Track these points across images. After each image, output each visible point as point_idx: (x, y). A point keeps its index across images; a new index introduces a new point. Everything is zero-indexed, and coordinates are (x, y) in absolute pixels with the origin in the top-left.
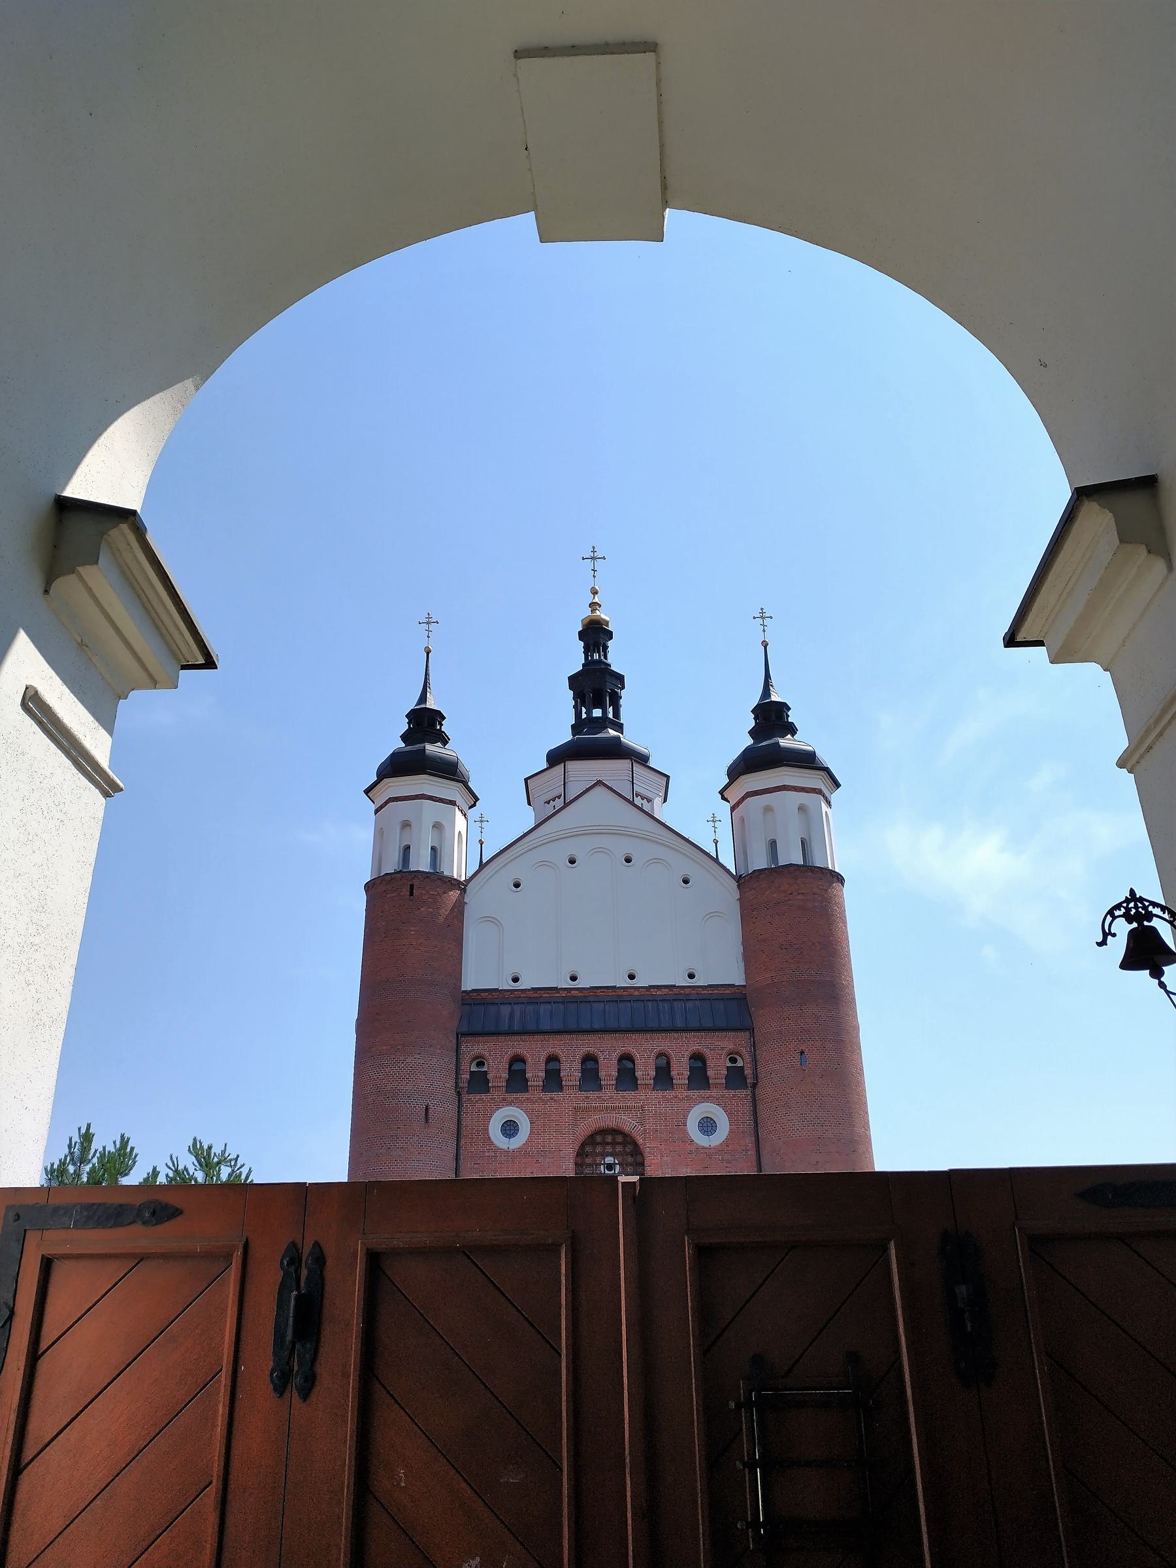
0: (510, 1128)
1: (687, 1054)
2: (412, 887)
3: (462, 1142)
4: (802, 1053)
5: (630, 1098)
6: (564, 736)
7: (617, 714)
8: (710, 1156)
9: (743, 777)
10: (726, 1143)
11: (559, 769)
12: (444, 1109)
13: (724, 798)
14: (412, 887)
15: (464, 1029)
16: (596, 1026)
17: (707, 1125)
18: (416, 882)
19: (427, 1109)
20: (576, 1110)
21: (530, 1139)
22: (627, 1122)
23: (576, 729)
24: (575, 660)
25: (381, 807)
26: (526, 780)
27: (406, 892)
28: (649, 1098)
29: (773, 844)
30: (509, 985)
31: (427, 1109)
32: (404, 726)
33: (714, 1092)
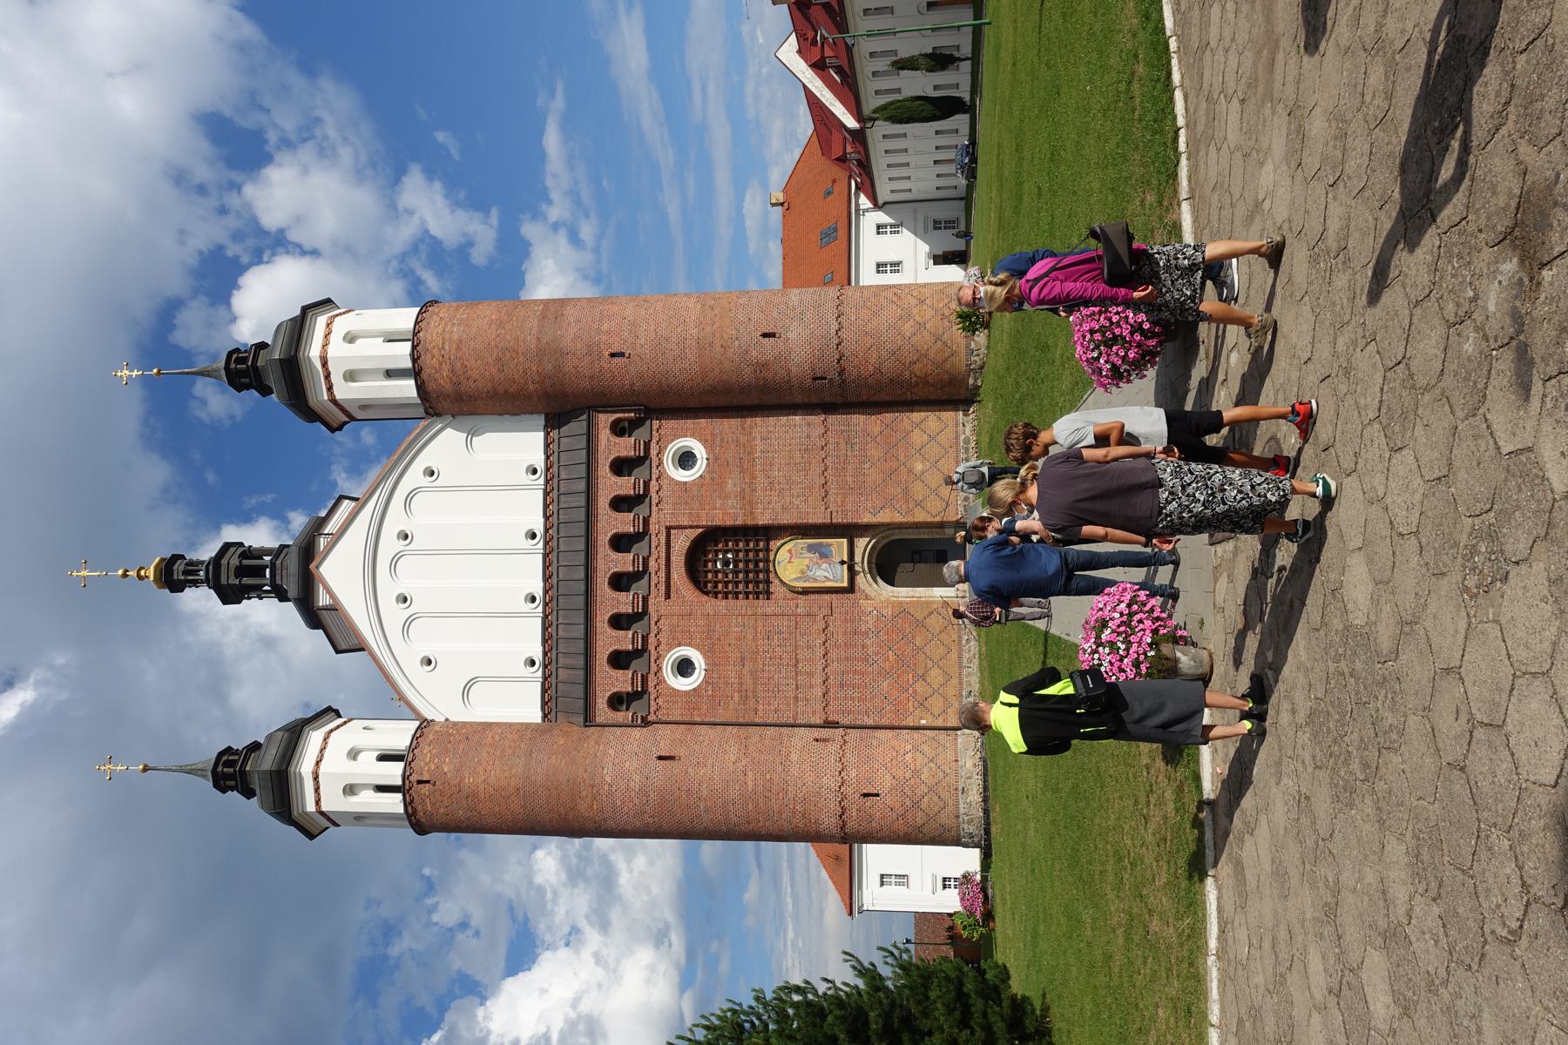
0: (684, 667)
1: (614, 479)
2: (419, 782)
3: (698, 719)
4: (613, 355)
5: (657, 538)
6: (290, 607)
7: (268, 552)
8: (716, 459)
9: (311, 403)
10: (704, 442)
11: (325, 615)
12: (664, 738)
13: (340, 428)
14: (419, 782)
15: (581, 719)
16: (582, 575)
17: (686, 460)
18: (414, 778)
19: (660, 758)
20: (668, 596)
21: (697, 647)
22: (681, 542)
23: (282, 596)
24: (199, 599)
25: (329, 819)
26: (338, 652)
27: (425, 789)
28: (660, 519)
29: (390, 374)
30: (537, 673)
31: (660, 758)
32: (234, 796)
33: (653, 452)
